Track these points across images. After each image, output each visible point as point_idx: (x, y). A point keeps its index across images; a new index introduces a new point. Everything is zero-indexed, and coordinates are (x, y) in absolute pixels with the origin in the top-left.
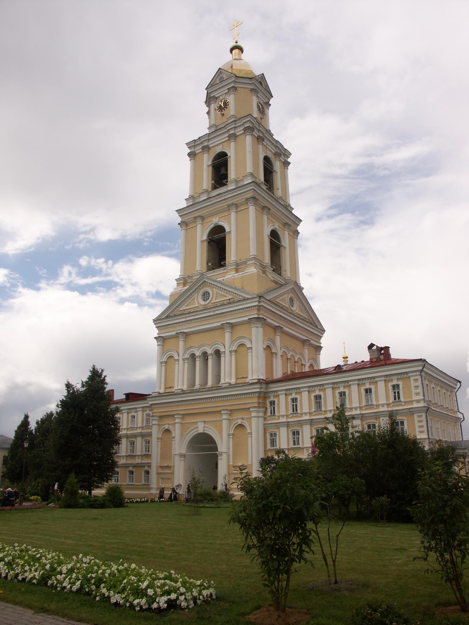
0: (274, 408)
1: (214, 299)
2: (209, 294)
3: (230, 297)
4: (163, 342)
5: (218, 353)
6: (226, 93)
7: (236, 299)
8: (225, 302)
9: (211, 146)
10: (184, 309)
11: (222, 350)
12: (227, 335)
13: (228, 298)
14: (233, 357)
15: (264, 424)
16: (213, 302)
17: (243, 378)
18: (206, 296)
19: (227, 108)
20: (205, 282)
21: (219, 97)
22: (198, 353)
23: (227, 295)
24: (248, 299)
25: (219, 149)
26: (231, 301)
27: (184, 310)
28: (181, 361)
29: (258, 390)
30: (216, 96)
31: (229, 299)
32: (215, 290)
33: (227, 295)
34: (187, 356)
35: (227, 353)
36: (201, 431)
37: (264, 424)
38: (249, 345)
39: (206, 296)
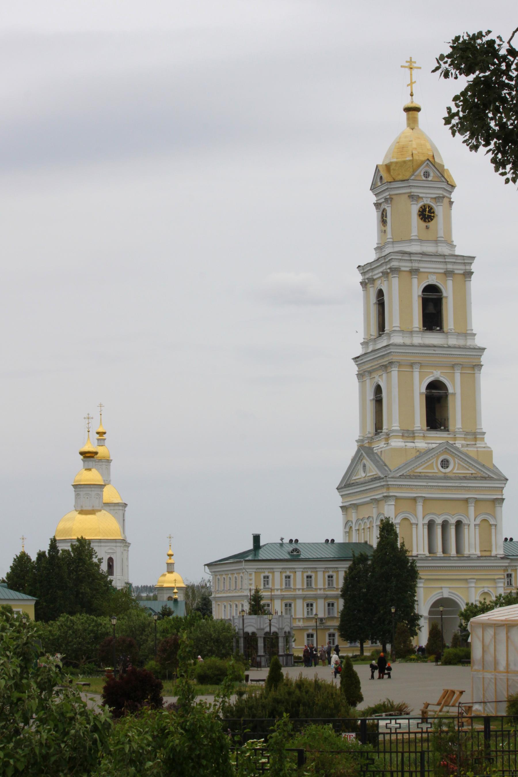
0: (510, 580)
1: (453, 468)
2: (448, 461)
3: (473, 472)
4: (395, 503)
5: (459, 524)
6: (432, 198)
8: (468, 475)
9: (421, 270)
11: (465, 521)
12: (472, 509)
13: (471, 472)
14: (477, 531)
16: (454, 472)
17: (485, 551)
18: (445, 464)
19: (432, 220)
21: (422, 198)
22: (439, 521)
23: (470, 469)
25: (432, 280)
27: (420, 473)
28: (420, 526)
29: (507, 564)
30: (421, 195)
31: (472, 474)
32: (456, 460)
33: (470, 469)
34: (426, 521)
36: (446, 595)
38: (492, 522)
39: (445, 464)
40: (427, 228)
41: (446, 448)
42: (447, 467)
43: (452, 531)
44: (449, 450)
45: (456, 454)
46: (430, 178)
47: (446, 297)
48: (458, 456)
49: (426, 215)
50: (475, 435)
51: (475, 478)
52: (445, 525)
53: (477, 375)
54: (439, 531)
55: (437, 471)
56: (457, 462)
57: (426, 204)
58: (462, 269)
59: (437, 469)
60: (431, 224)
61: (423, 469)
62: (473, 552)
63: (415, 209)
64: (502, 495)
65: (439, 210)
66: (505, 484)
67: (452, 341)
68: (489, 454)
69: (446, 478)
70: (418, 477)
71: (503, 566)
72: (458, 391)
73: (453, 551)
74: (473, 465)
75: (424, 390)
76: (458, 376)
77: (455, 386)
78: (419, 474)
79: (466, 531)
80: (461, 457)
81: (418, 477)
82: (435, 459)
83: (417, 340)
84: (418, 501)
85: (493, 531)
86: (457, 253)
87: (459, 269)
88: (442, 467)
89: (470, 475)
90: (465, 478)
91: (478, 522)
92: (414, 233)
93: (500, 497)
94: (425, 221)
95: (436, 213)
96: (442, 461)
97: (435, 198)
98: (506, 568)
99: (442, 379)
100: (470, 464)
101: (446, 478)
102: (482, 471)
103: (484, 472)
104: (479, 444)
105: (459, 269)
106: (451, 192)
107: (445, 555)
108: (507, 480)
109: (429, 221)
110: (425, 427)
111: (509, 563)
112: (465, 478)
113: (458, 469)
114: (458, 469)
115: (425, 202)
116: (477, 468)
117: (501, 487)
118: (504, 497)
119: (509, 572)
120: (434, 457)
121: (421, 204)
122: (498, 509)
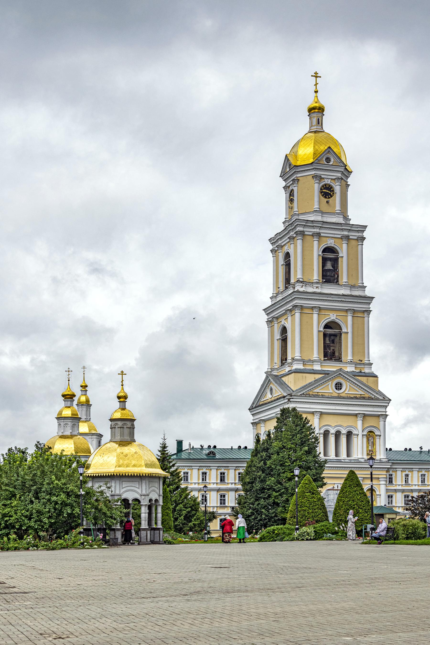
2: (341, 384)
3: (363, 393)
5: (349, 435)
6: (332, 179)
7: (367, 396)
9: (322, 235)
10: (318, 391)
11: (355, 432)
15: (386, 489)
18: (339, 386)
19: (331, 196)
20: (340, 374)
21: (324, 178)
22: (333, 431)
25: (331, 243)
27: (318, 393)
29: (389, 467)
31: (361, 395)
35: (360, 436)
37: (386, 489)
39: (339, 386)
40: (327, 202)
41: (340, 374)
42: (341, 389)
43: (343, 440)
44: (342, 375)
45: (348, 379)
46: (331, 163)
47: (342, 257)
48: (350, 380)
49: (327, 192)
51: (364, 398)
52: (338, 435)
53: (366, 319)
54: (332, 439)
57: (327, 184)
58: (356, 235)
60: (330, 200)
62: (360, 456)
63: (316, 187)
64: (386, 412)
65: (337, 189)
66: (389, 403)
69: (339, 397)
70: (316, 396)
71: (386, 468)
72: (350, 330)
73: (343, 455)
74: (362, 388)
76: (350, 318)
77: (348, 325)
78: (317, 393)
79: (354, 439)
80: (352, 381)
81: (316, 396)
82: (330, 382)
84: (315, 415)
86: (351, 222)
88: (336, 389)
89: (360, 396)
90: (356, 398)
91: (365, 433)
92: (316, 206)
93: (384, 413)
94: (325, 197)
96: (336, 384)
97: (334, 179)
98: (388, 470)
99: (337, 321)
100: (360, 387)
101: (339, 397)
102: (369, 392)
103: (371, 394)
105: (353, 235)
106: (347, 177)
108: (390, 400)
109: (329, 198)
111: (391, 466)
112: (356, 398)
113: (348, 391)
114: (348, 391)
115: (327, 183)
116: (366, 390)
117: (385, 406)
118: (387, 414)
119: (391, 473)
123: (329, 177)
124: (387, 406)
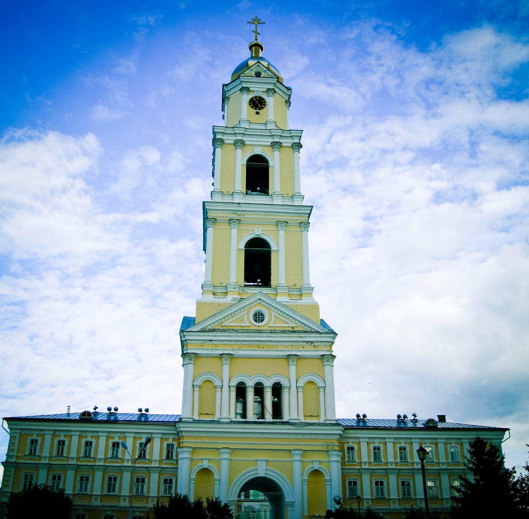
2: (262, 315)
18: (259, 317)
24: (318, 332)
25: (258, 151)
26: (295, 329)
39: (259, 317)
42: (262, 321)
47: (273, 167)
50: (302, 290)
55: (249, 325)
56: (273, 316)
59: (249, 321)
60: (260, 111)
61: (232, 322)
66: (334, 338)
67: (277, 201)
68: (315, 307)
75: (242, 246)
83: (236, 201)
85: (322, 394)
87: (287, 142)
88: (256, 321)
91: (301, 383)
95: (267, 102)
96: (255, 315)
99: (264, 237)
103: (309, 327)
104: (305, 300)
107: (245, 420)
108: (336, 334)
110: (242, 282)
112: (282, 332)
115: (257, 95)
120: (246, 308)
121: (251, 95)
122: (327, 368)
123: (258, 89)
124: (333, 343)
